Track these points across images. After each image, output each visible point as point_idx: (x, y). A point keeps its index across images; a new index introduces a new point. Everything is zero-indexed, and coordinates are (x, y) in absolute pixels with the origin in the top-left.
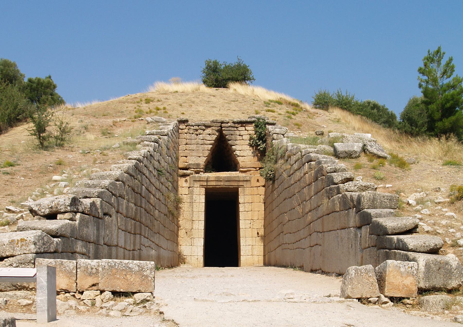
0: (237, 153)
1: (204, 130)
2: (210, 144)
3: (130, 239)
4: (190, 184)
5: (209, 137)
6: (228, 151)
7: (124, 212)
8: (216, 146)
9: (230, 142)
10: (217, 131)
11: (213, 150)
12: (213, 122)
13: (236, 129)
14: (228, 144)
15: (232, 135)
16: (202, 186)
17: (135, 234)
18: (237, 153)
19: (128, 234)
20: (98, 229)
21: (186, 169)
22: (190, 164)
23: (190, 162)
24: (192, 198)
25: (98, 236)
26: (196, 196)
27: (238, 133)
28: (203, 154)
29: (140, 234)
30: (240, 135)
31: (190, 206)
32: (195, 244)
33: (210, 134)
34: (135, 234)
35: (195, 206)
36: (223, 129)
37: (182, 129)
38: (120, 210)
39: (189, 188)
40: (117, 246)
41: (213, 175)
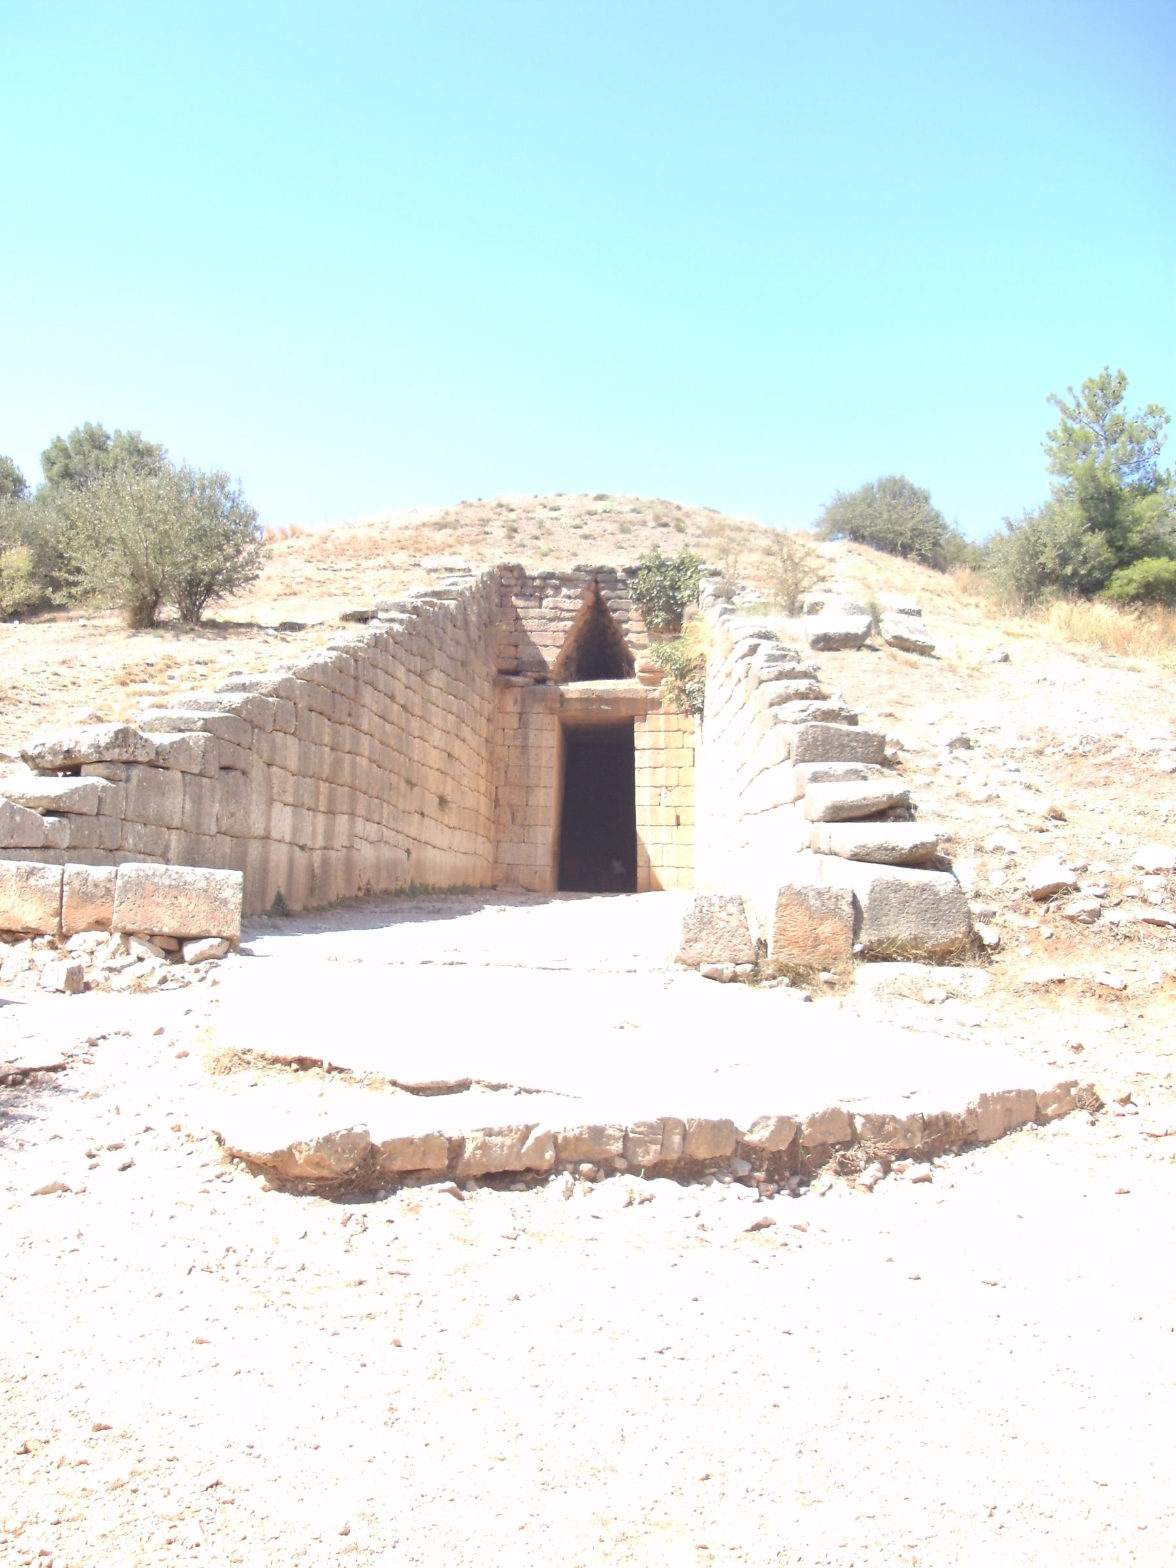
0: (631, 637)
1: (557, 589)
3: (314, 825)
4: (523, 706)
5: (568, 604)
6: (614, 634)
7: (293, 763)
8: (586, 622)
9: (615, 615)
10: (588, 589)
11: (580, 630)
14: (611, 620)
15: (620, 598)
16: (552, 712)
17: (334, 814)
19: (305, 812)
20: (198, 801)
21: (516, 673)
22: (523, 663)
24: (525, 738)
25: (198, 813)
28: (554, 639)
29: (352, 814)
31: (522, 753)
33: (569, 597)
34: (331, 812)
35: (532, 754)
37: (509, 586)
38: (278, 761)
39: (520, 714)
40: (266, 837)
41: (575, 689)
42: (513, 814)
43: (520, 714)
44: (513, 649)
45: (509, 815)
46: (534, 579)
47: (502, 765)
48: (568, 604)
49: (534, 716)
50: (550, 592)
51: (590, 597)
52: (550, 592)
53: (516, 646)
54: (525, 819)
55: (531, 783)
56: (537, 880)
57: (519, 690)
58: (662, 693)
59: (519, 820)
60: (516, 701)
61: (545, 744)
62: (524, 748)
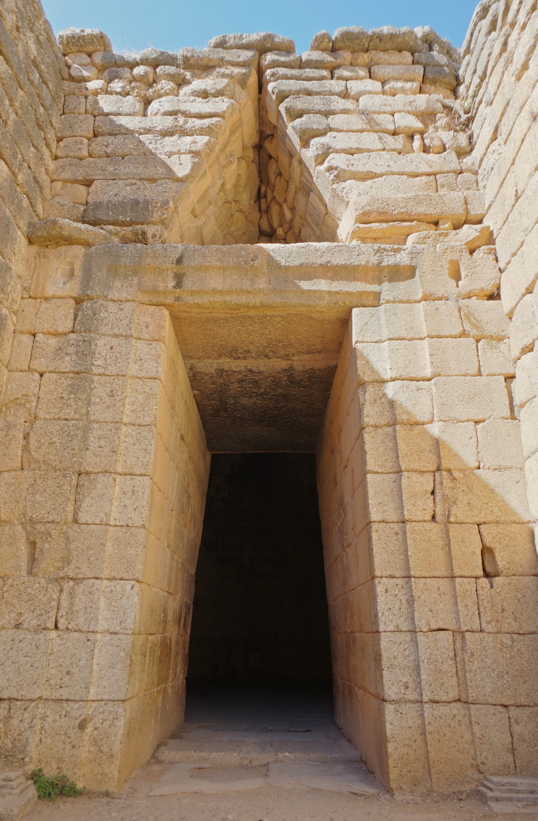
1: (181, 83)
2: (208, 131)
4: (86, 282)
5: (200, 106)
12: (222, 44)
13: (325, 73)
15: (309, 93)
18: (334, 163)
23: (104, 198)
24: (85, 352)
26: (115, 341)
27: (337, 86)
30: (345, 95)
31: (73, 389)
32: (81, 621)
33: (204, 95)
35: (100, 391)
36: (269, 72)
42: (33, 544)
43: (78, 301)
44: (82, 188)
45: (24, 550)
46: (132, 65)
47: (22, 417)
48: (200, 106)
49: (112, 307)
50: (165, 85)
51: (246, 99)
52: (165, 85)
53: (88, 184)
54: (67, 560)
55: (90, 462)
56: (85, 751)
57: (80, 250)
58: (414, 254)
59: (48, 564)
60: (72, 275)
61: (133, 369)
62: (81, 376)
